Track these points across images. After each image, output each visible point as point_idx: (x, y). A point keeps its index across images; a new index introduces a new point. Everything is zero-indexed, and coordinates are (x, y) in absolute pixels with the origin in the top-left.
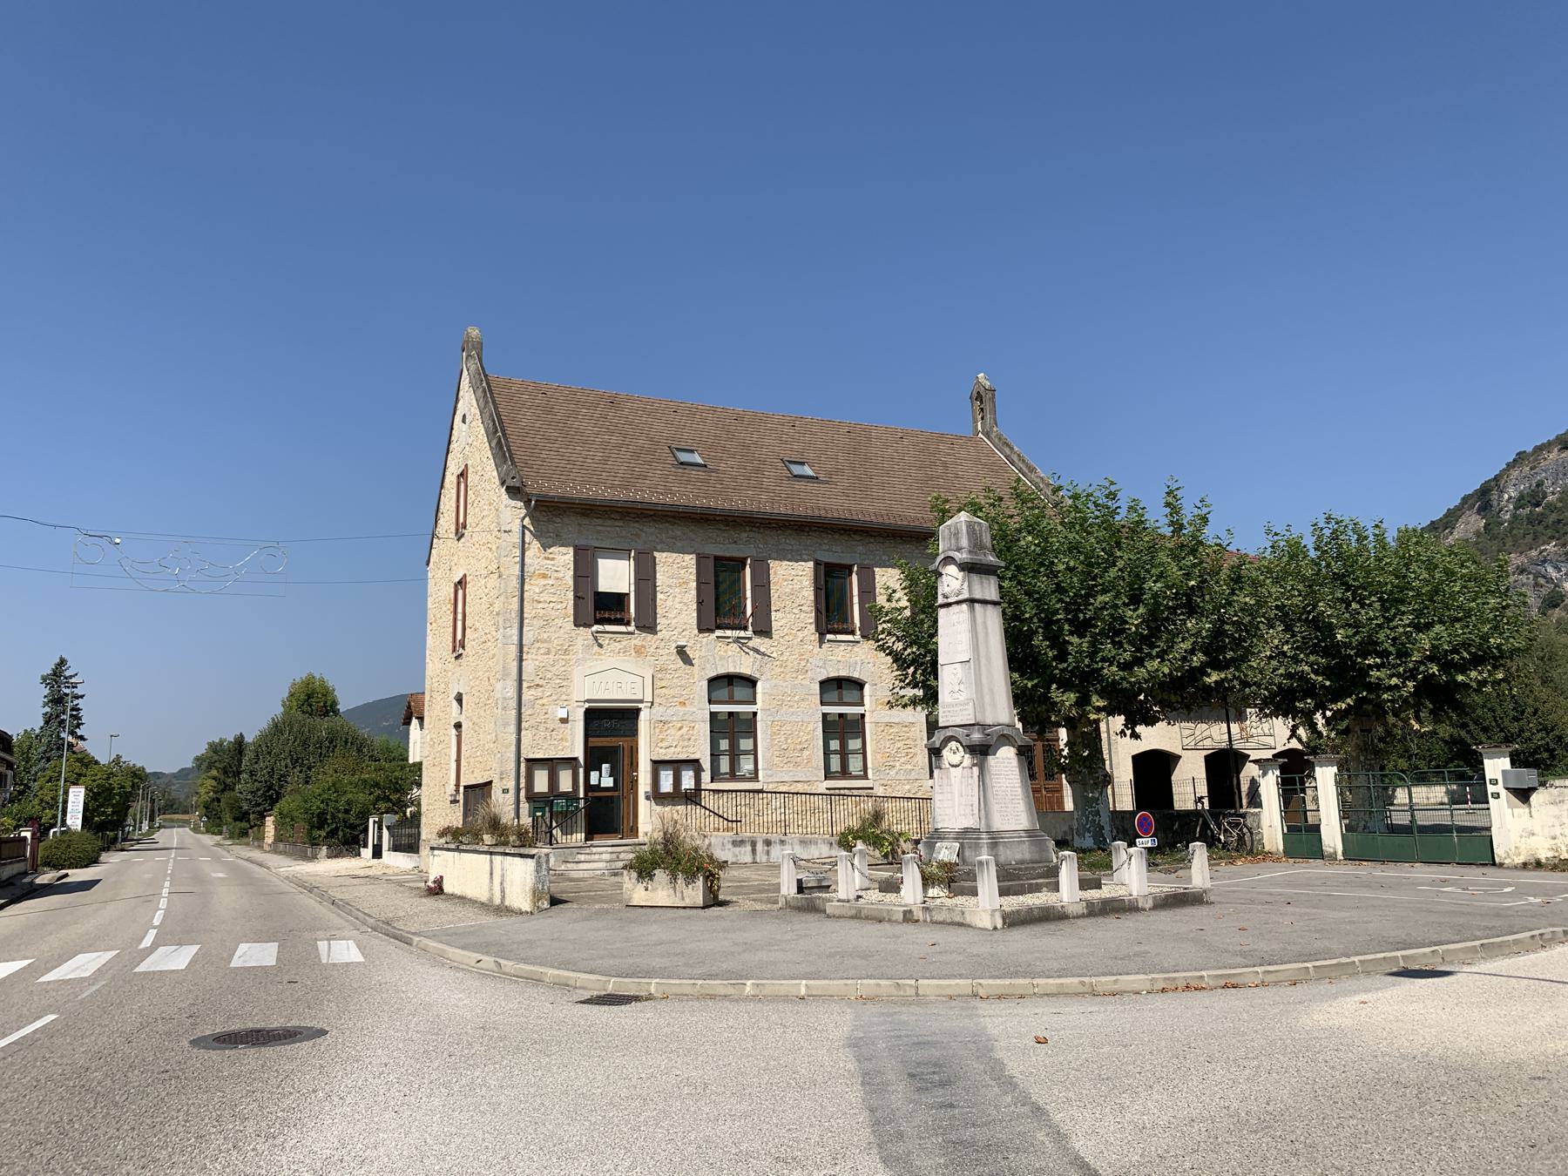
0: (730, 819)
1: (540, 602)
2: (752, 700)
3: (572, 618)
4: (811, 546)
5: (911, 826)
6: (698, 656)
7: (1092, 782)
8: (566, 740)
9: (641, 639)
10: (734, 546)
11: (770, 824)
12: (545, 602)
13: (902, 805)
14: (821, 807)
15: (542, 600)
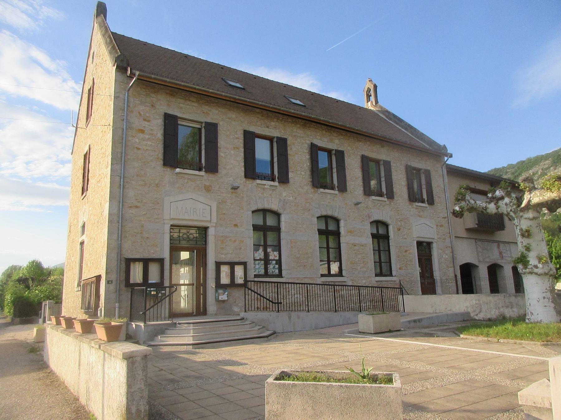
4: (311, 136)
10: (267, 129)
11: (291, 305)
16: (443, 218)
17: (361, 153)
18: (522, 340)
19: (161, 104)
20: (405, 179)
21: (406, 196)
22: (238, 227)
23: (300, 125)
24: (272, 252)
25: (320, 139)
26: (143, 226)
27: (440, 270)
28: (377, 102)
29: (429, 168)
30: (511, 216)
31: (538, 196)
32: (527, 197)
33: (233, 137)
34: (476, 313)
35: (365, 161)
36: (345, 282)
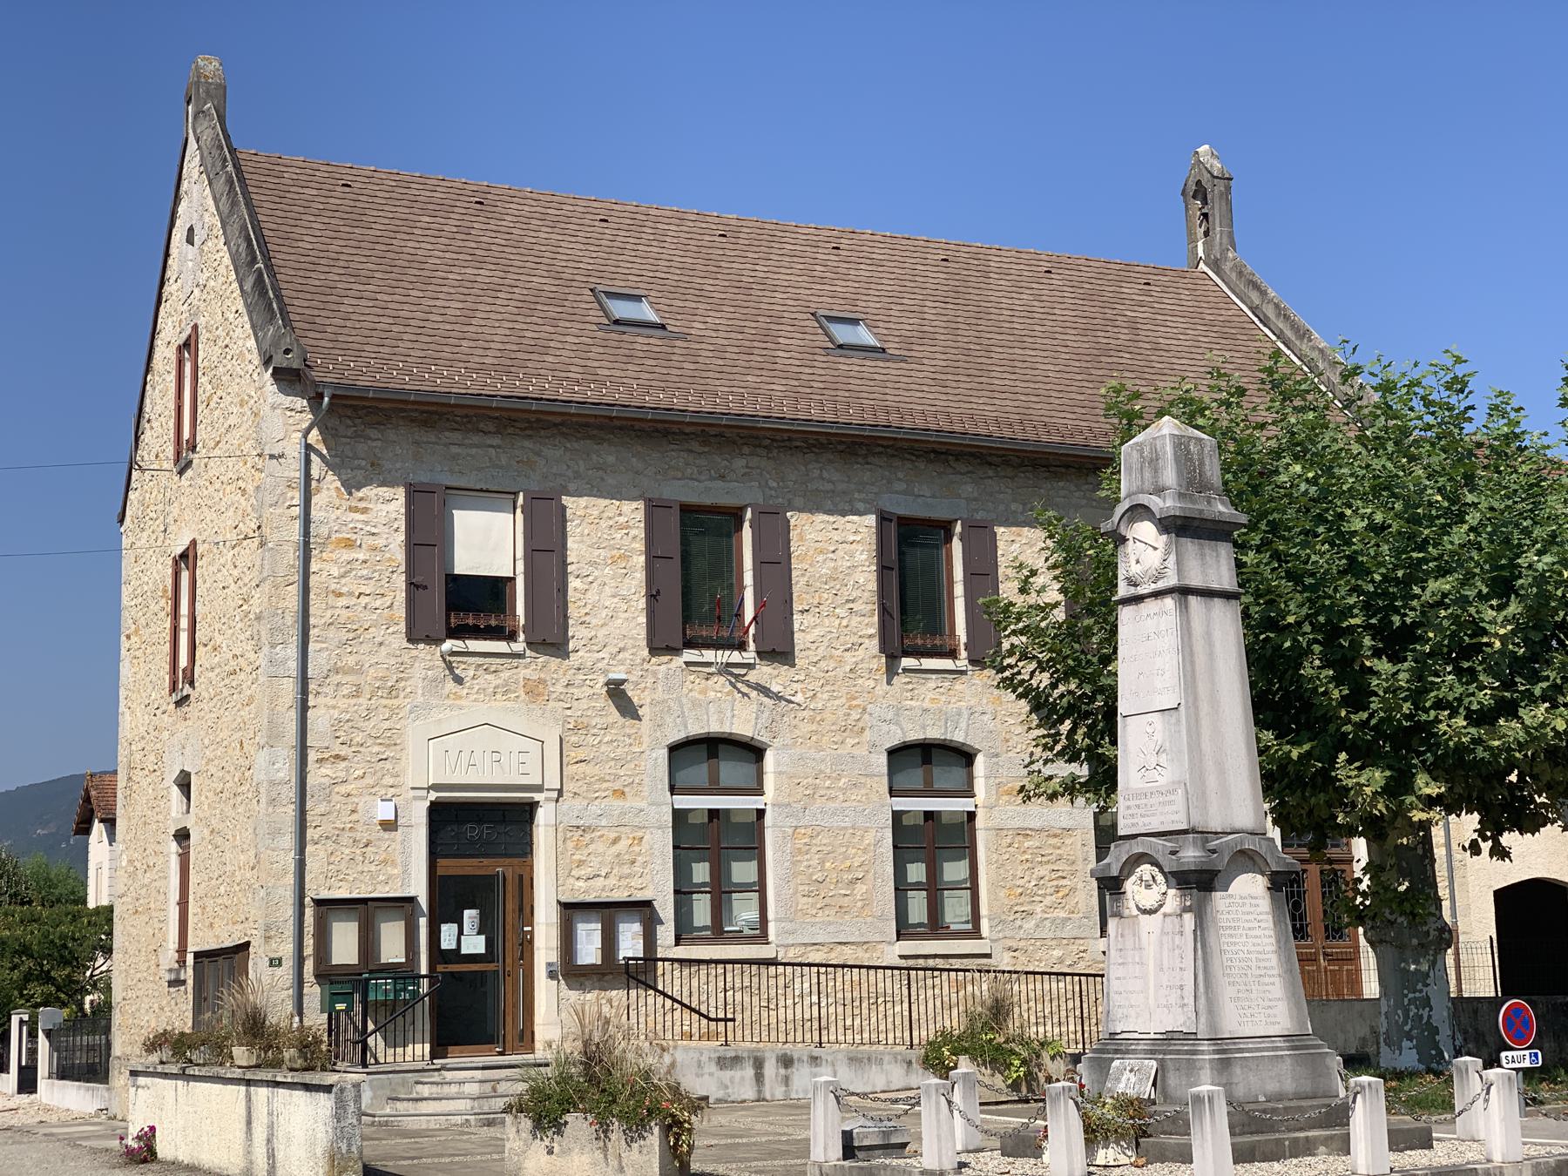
0: (713, 1015)
1: (340, 595)
2: (755, 786)
3: (402, 627)
4: (873, 484)
5: (1064, 1029)
6: (648, 700)
7: (1415, 941)
8: (393, 864)
9: (538, 666)
10: (720, 484)
11: (790, 1026)
12: (351, 594)
13: (1047, 987)
14: (889, 991)
15: (344, 590)
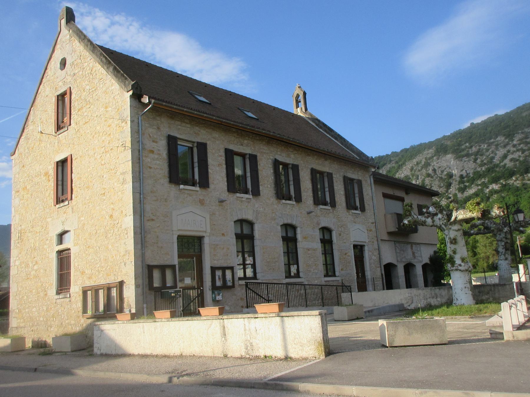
4: (273, 152)
10: (242, 147)
16: (372, 223)
17: (310, 167)
18: (456, 316)
19: (164, 126)
20: (343, 189)
21: (344, 204)
22: (225, 236)
23: (265, 142)
24: (248, 257)
25: (280, 155)
26: (158, 237)
27: (371, 270)
28: (306, 109)
29: (360, 178)
30: (443, 228)
31: (462, 214)
32: (454, 214)
33: (218, 154)
34: (408, 304)
35: (314, 172)
36: (303, 282)
